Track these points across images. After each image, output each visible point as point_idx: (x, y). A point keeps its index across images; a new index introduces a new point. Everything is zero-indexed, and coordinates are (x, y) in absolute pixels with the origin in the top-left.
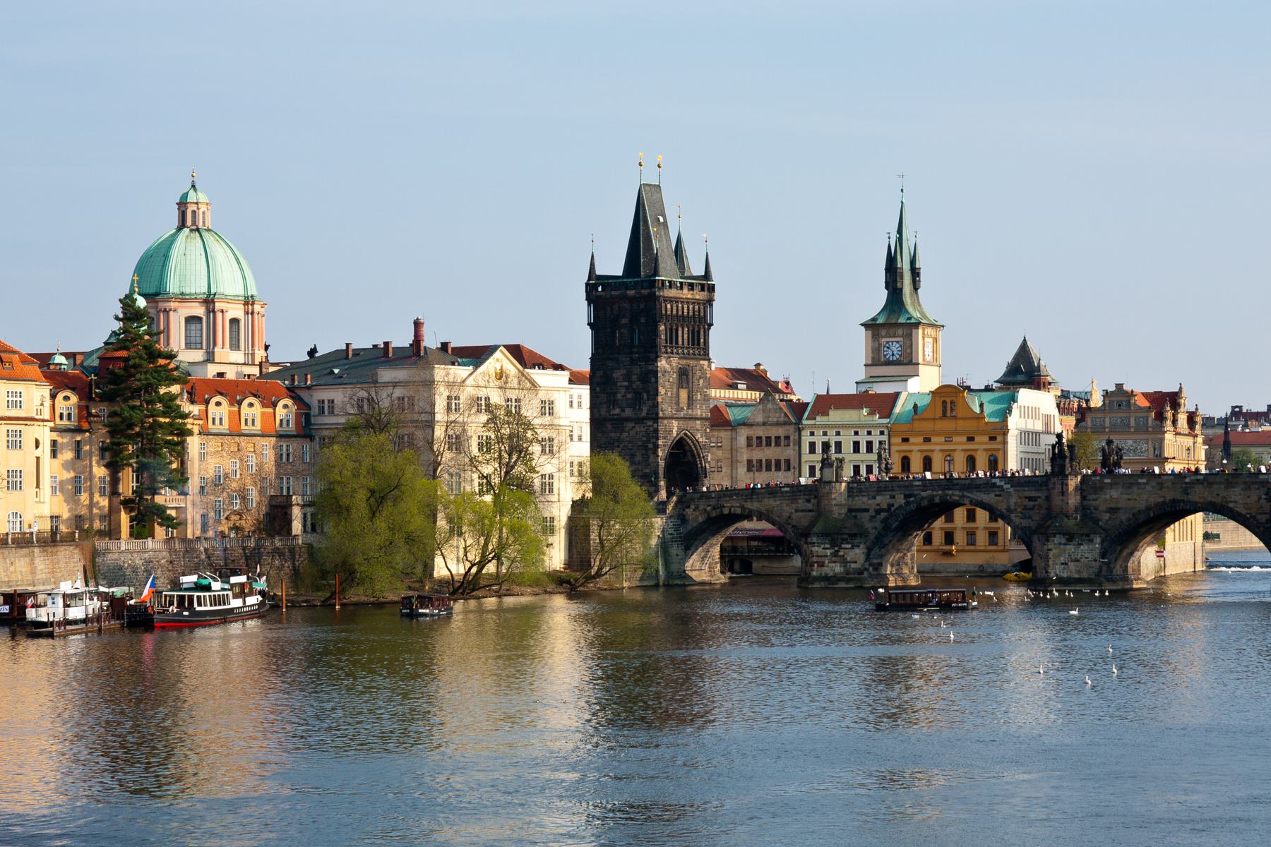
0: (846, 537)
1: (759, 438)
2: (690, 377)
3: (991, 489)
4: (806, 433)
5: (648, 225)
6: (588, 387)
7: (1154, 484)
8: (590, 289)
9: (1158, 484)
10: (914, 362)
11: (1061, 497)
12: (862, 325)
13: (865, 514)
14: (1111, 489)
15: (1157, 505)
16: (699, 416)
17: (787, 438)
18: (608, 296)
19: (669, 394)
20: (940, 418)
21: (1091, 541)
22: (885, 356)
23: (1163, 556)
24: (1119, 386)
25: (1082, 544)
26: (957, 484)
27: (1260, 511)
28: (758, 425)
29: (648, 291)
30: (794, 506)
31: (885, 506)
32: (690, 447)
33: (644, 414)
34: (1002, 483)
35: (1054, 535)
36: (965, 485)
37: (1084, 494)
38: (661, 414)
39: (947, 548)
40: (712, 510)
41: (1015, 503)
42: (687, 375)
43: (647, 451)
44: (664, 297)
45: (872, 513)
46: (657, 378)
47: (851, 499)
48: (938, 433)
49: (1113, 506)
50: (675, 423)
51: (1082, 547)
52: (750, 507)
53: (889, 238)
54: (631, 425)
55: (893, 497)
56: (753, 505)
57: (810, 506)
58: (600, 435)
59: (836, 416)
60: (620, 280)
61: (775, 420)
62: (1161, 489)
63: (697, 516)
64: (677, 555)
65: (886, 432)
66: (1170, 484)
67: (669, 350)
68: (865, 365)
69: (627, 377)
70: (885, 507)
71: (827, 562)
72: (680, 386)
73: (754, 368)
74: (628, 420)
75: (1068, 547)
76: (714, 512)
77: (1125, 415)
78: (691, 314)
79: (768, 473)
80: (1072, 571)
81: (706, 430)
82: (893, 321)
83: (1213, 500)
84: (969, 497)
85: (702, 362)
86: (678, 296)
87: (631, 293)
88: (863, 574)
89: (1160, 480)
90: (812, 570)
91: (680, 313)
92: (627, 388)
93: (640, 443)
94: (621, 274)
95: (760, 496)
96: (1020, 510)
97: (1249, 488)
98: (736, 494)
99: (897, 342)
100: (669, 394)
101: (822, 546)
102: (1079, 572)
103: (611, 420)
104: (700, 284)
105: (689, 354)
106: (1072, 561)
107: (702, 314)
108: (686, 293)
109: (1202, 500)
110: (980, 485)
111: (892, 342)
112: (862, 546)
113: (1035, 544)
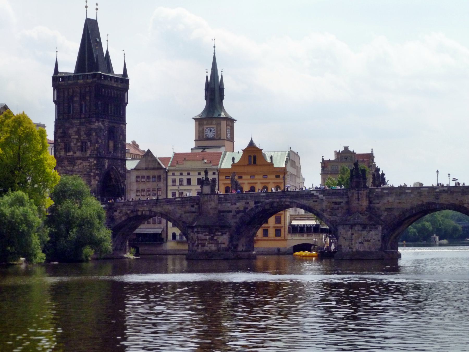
0: (218, 228)
4: (170, 174)
7: (416, 193)
9: (418, 193)
10: (222, 138)
11: (357, 202)
12: (193, 118)
15: (418, 206)
16: (120, 158)
17: (159, 177)
18: (66, 84)
19: (103, 142)
20: (248, 165)
21: (376, 228)
22: (206, 135)
24: (346, 148)
25: (371, 231)
26: (289, 195)
28: (143, 169)
29: (91, 80)
30: (184, 209)
31: (242, 209)
33: (88, 155)
34: (318, 194)
35: (355, 225)
36: (293, 195)
37: (371, 200)
40: (130, 213)
41: (326, 206)
43: (90, 177)
45: (233, 213)
48: (246, 174)
50: (107, 161)
51: (371, 232)
52: (155, 210)
53: (207, 72)
54: (80, 161)
55: (248, 203)
56: (158, 209)
57: (193, 209)
61: (152, 166)
62: (420, 196)
63: (121, 217)
66: (426, 193)
67: (103, 117)
69: (78, 133)
71: (206, 243)
72: (109, 139)
74: (78, 158)
75: (363, 232)
82: (211, 116)
83: (454, 202)
84: (296, 202)
87: (81, 82)
90: (198, 249)
91: (110, 95)
92: (77, 140)
93: (85, 173)
95: (162, 204)
99: (213, 128)
100: (103, 142)
101: (204, 234)
103: (67, 158)
106: (366, 241)
109: (447, 203)
110: (304, 195)
111: (210, 128)
112: (228, 233)
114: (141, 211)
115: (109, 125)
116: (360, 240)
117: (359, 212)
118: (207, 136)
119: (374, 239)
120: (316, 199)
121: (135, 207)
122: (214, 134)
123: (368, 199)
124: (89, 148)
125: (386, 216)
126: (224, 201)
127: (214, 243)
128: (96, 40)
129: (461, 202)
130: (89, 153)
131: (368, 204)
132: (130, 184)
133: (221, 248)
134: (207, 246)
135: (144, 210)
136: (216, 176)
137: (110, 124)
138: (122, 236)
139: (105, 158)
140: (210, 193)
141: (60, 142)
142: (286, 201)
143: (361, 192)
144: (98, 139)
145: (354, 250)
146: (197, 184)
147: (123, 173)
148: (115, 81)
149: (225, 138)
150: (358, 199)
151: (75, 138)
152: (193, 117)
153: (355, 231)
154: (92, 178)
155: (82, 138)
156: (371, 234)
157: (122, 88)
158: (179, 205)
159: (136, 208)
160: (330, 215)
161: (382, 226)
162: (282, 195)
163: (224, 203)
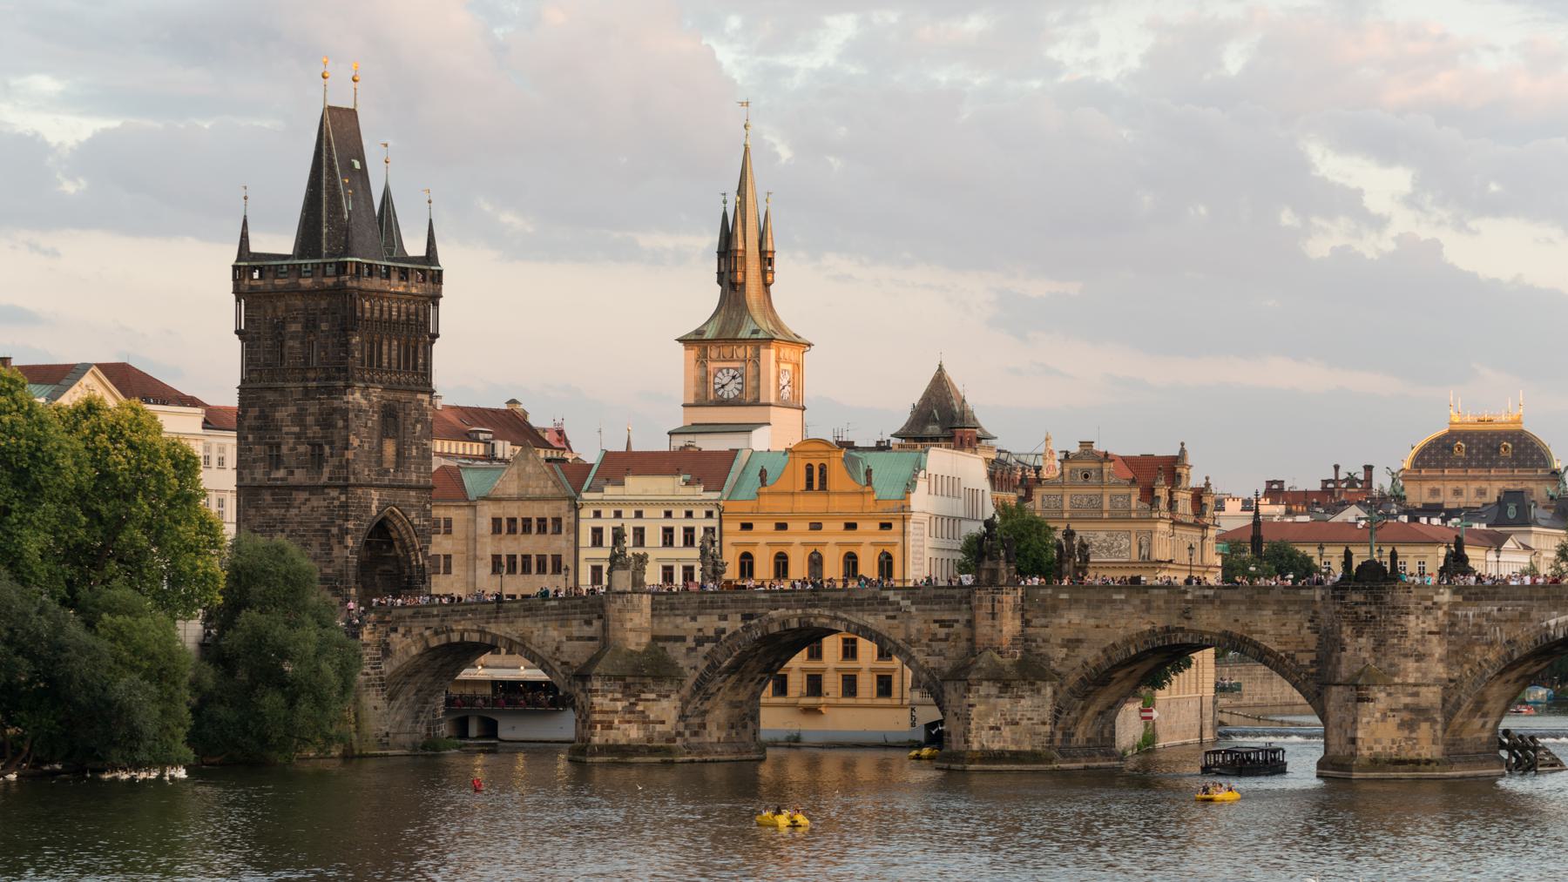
1: (512, 521)
2: (401, 419)
3: (881, 608)
4: (587, 513)
5: (336, 174)
6: (234, 434)
7: (1137, 602)
8: (240, 273)
9: (1143, 602)
10: (762, 401)
11: (990, 622)
12: (679, 340)
13: (678, 644)
14: (1070, 609)
16: (414, 483)
17: (557, 521)
18: (269, 287)
19: (366, 446)
23: (1151, 718)
25: (1022, 697)
26: (826, 599)
27: (1302, 648)
28: (510, 499)
29: (335, 280)
31: (711, 633)
32: (399, 534)
33: (324, 479)
37: (1028, 616)
38: (352, 480)
39: (812, 701)
41: (918, 630)
42: (395, 417)
43: (329, 539)
44: (360, 290)
45: (690, 643)
46: (346, 420)
47: (656, 621)
49: (1074, 637)
50: (375, 494)
51: (1023, 701)
52: (493, 631)
53: (725, 202)
54: (302, 496)
56: (499, 629)
57: (588, 631)
58: (252, 512)
59: (636, 486)
60: (288, 262)
61: (538, 491)
63: (409, 646)
64: (376, 708)
65: (716, 514)
66: (1161, 603)
67: (367, 376)
68: (684, 406)
69: (299, 418)
70: (711, 633)
71: (616, 722)
72: (384, 435)
73: (505, 407)
74: (298, 488)
75: (1001, 700)
76: (435, 638)
77: (1098, 491)
78: (403, 317)
79: (526, 576)
80: (1004, 741)
81: (424, 506)
83: (1230, 629)
84: (845, 619)
85: (420, 396)
86: (382, 288)
87: (306, 282)
88: (675, 741)
89: (1146, 596)
91: (386, 316)
92: (298, 436)
93: (318, 526)
94: (291, 253)
96: (925, 641)
97: (1285, 610)
98: (472, 611)
100: (366, 446)
101: (610, 696)
102: (1015, 741)
103: (270, 487)
104: (419, 270)
105: (399, 383)
106: (1007, 724)
107: (421, 319)
108: (396, 285)
110: (864, 599)
111: (728, 369)
112: (673, 696)
113: (947, 697)
114: (458, 630)
115: (382, 397)
116: (991, 722)
117: (994, 649)
118: (720, 393)
119: (1029, 719)
120: (893, 610)
121: (443, 621)
122: (740, 387)
123: (1018, 614)
124: (327, 462)
125: (1063, 659)
126: (668, 612)
127: (635, 722)
128: (352, 165)
129: (1246, 628)
130: (328, 475)
131: (1019, 629)
132: (475, 539)
133: (656, 734)
134: (619, 729)
135: (465, 630)
136: (713, 523)
137: (386, 395)
138: (415, 694)
139: (371, 486)
140: (630, 589)
141: (254, 443)
142: (820, 615)
143: (998, 596)
144: (351, 437)
145: (975, 746)
146: (661, 545)
147: (424, 526)
148: (401, 279)
149: (772, 401)
150: (993, 615)
151: (294, 433)
152: (680, 335)
153: (979, 696)
154: (333, 541)
155: (310, 433)
156: (1022, 706)
157: (421, 296)
158: (554, 617)
159: (446, 624)
160: (928, 655)
161: (1052, 685)
162: (809, 600)
163: (666, 615)
